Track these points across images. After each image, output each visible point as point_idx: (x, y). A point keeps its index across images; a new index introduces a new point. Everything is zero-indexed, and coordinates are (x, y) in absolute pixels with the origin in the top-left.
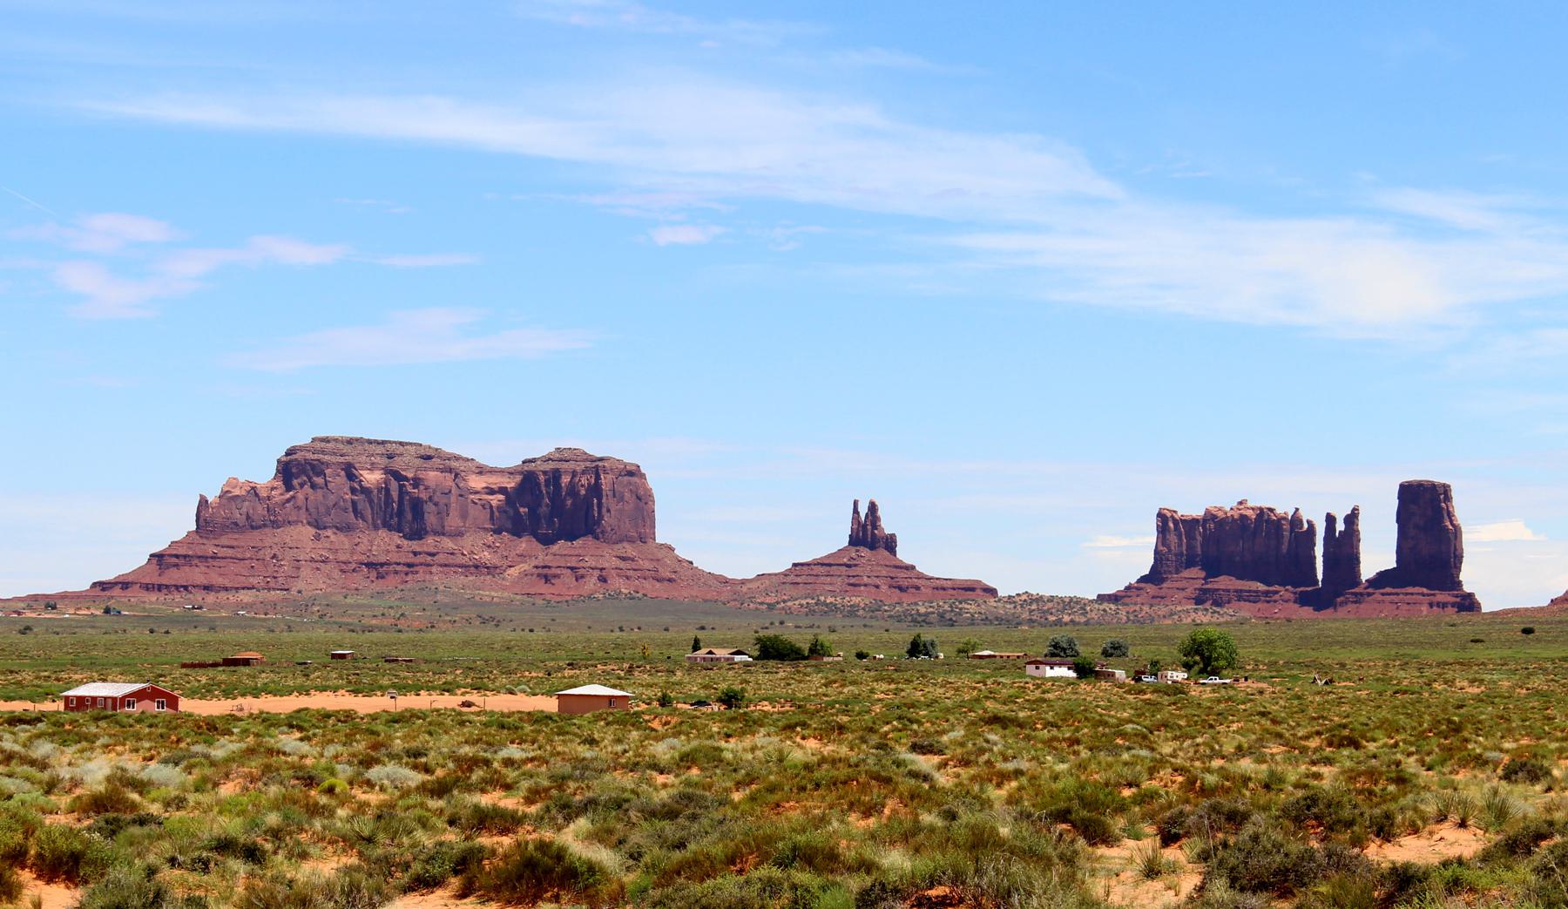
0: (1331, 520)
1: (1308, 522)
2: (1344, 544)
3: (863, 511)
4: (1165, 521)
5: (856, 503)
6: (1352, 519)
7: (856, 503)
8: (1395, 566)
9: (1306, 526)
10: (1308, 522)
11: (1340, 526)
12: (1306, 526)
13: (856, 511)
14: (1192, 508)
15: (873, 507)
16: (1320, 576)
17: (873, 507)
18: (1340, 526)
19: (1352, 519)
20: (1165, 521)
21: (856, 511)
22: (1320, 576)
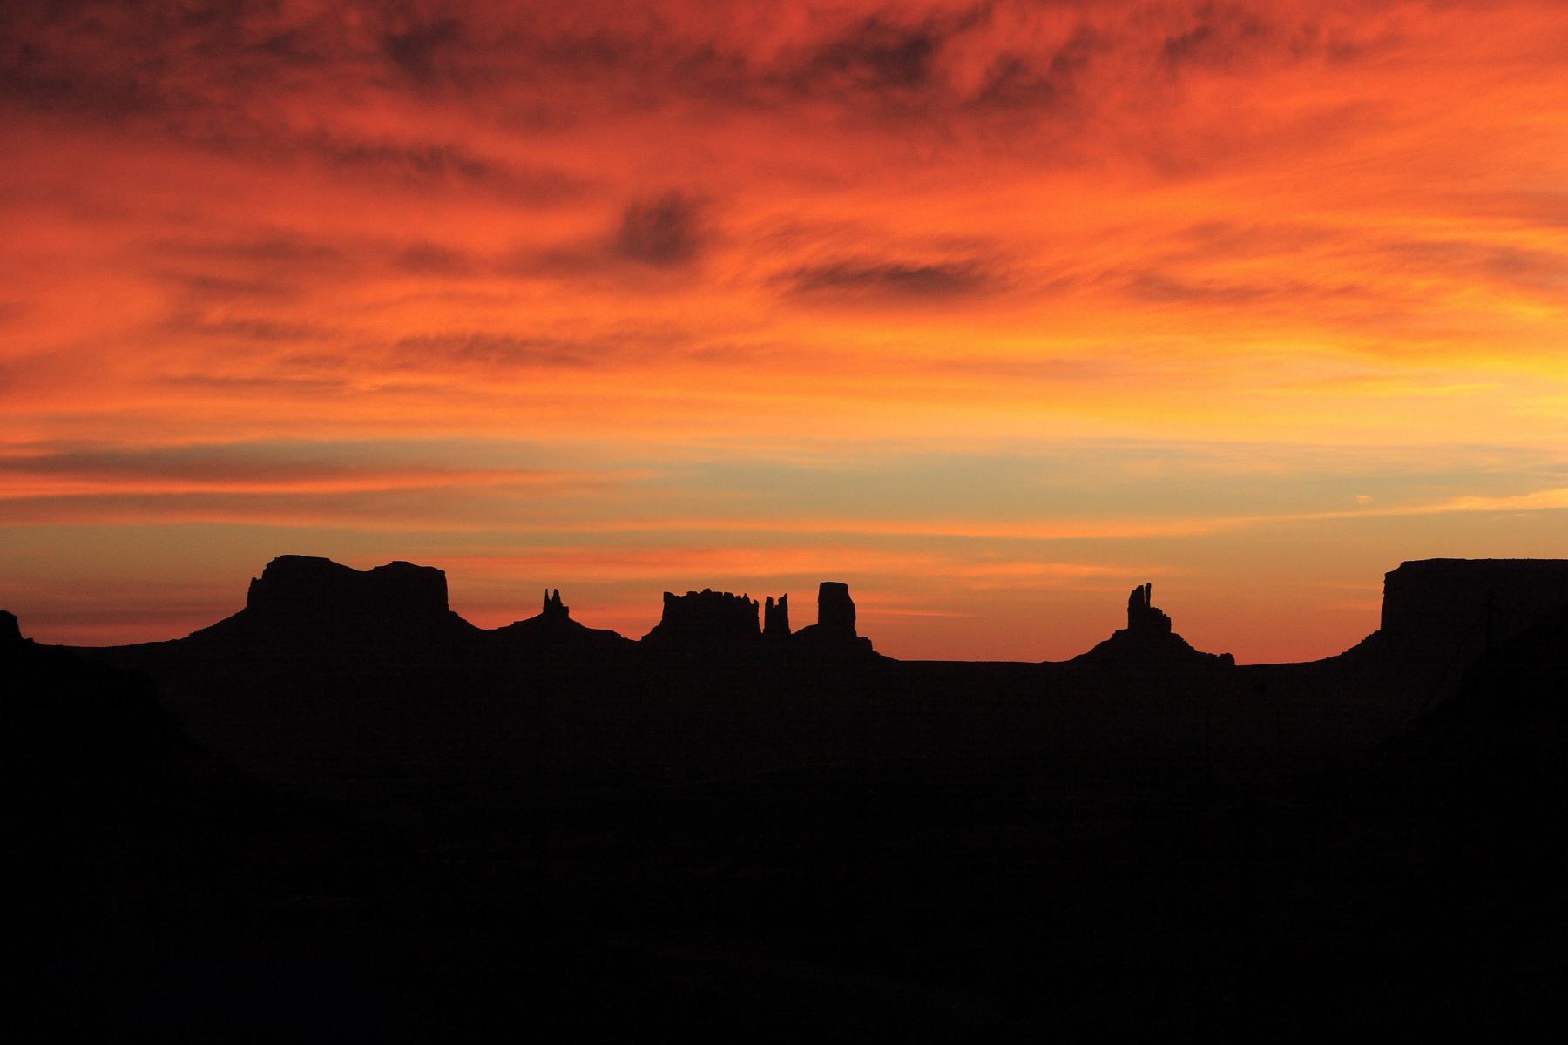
0: (769, 600)
1: (754, 601)
2: (778, 611)
3: (551, 597)
4: (668, 597)
5: (547, 590)
6: (783, 600)
7: (547, 590)
8: (814, 621)
9: (752, 603)
10: (754, 601)
11: (776, 603)
12: (752, 603)
13: (547, 596)
14: (681, 593)
15: (556, 592)
16: (762, 626)
17: (556, 592)
18: (776, 603)
19: (783, 600)
20: (668, 597)
21: (547, 596)
22: (762, 626)
